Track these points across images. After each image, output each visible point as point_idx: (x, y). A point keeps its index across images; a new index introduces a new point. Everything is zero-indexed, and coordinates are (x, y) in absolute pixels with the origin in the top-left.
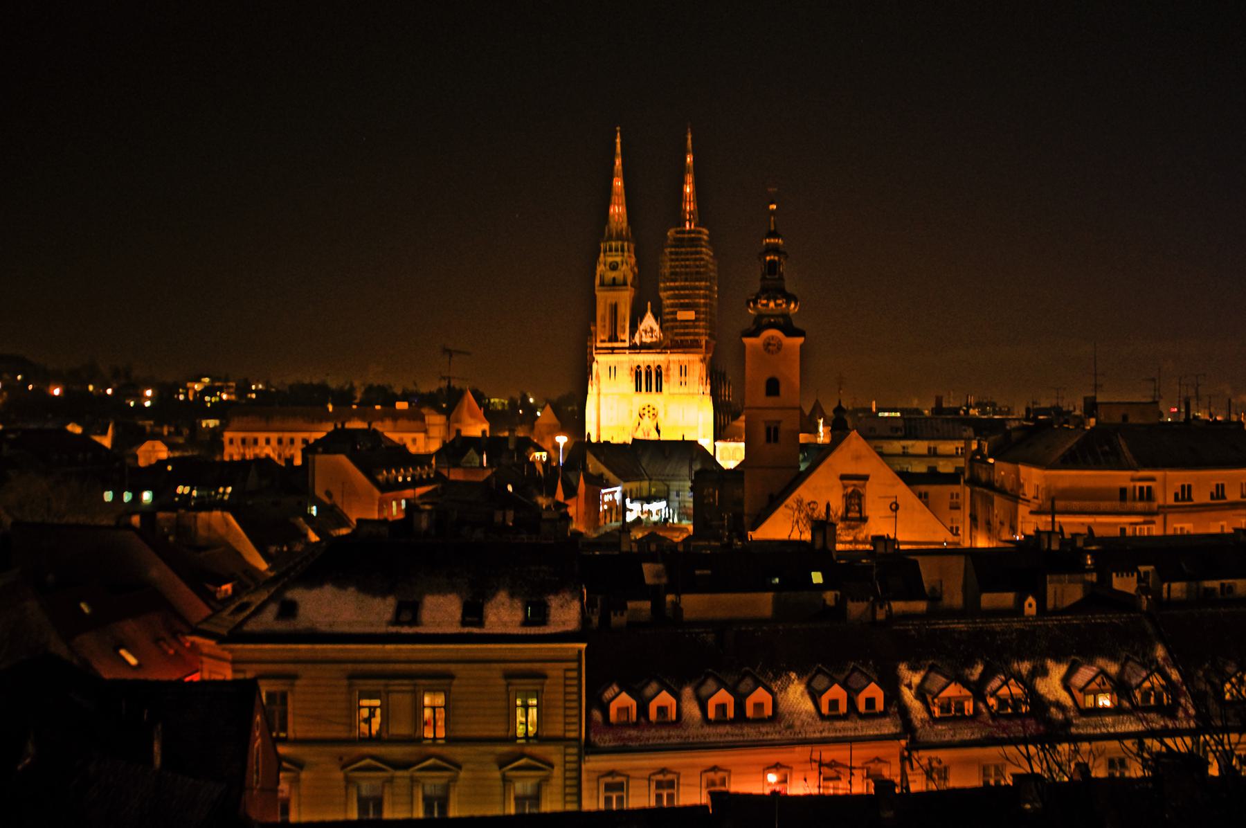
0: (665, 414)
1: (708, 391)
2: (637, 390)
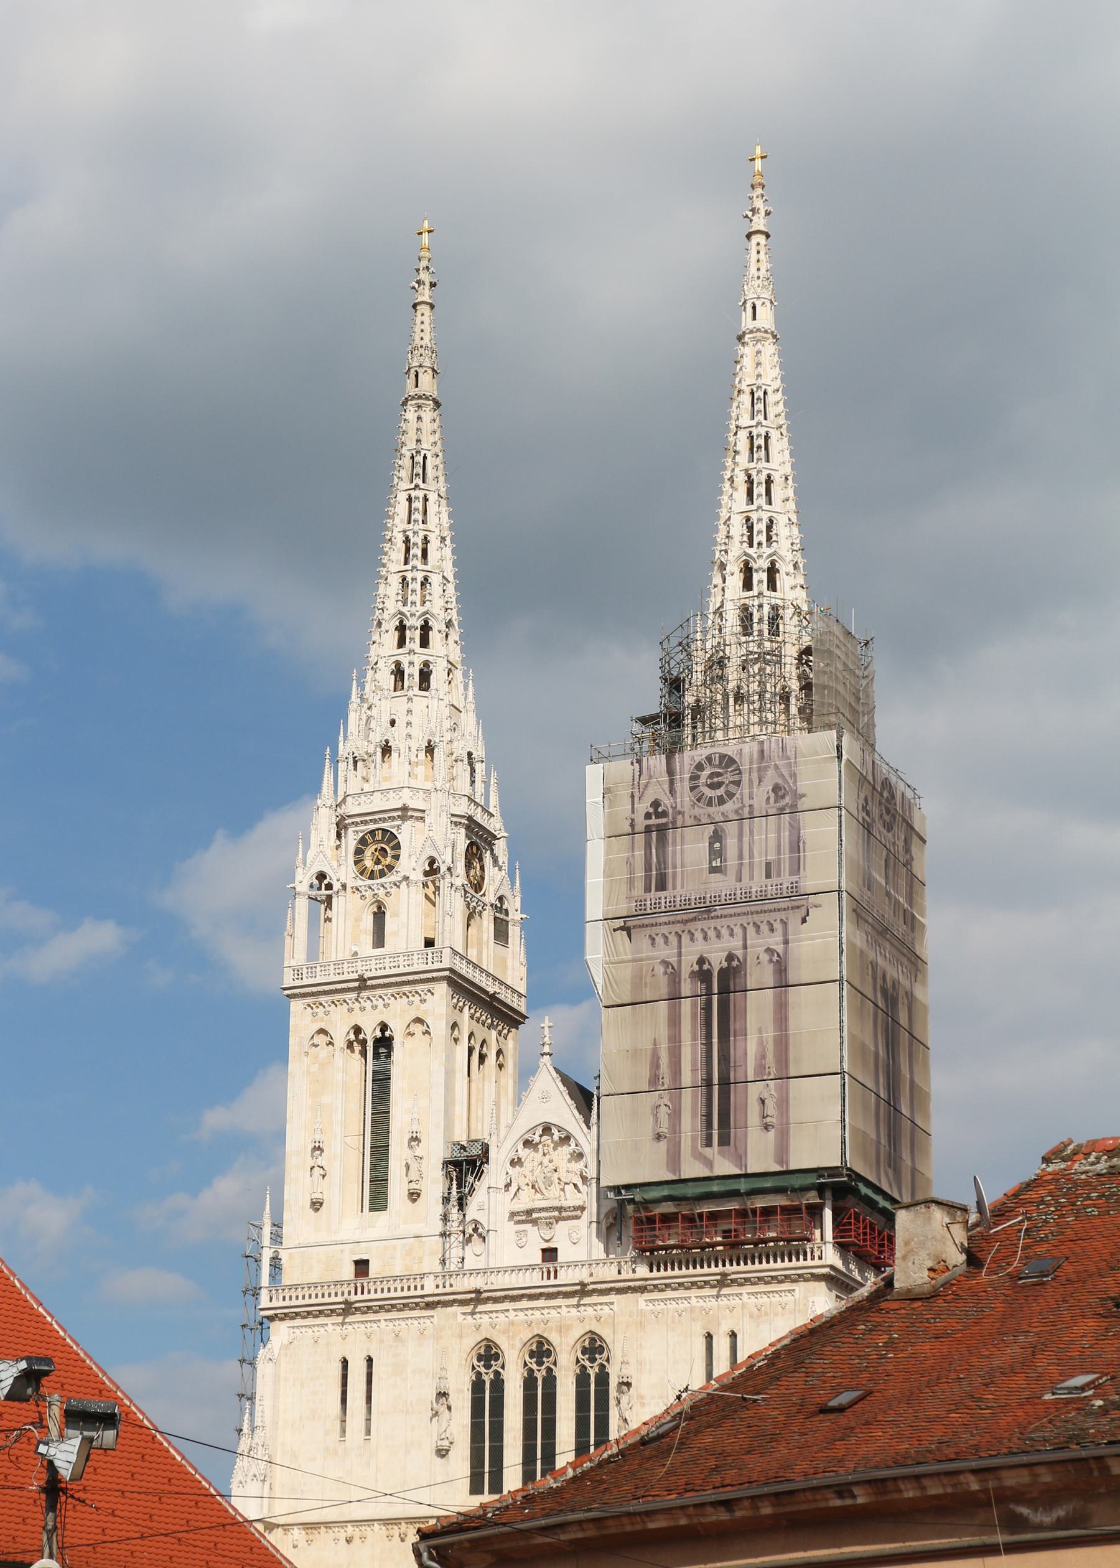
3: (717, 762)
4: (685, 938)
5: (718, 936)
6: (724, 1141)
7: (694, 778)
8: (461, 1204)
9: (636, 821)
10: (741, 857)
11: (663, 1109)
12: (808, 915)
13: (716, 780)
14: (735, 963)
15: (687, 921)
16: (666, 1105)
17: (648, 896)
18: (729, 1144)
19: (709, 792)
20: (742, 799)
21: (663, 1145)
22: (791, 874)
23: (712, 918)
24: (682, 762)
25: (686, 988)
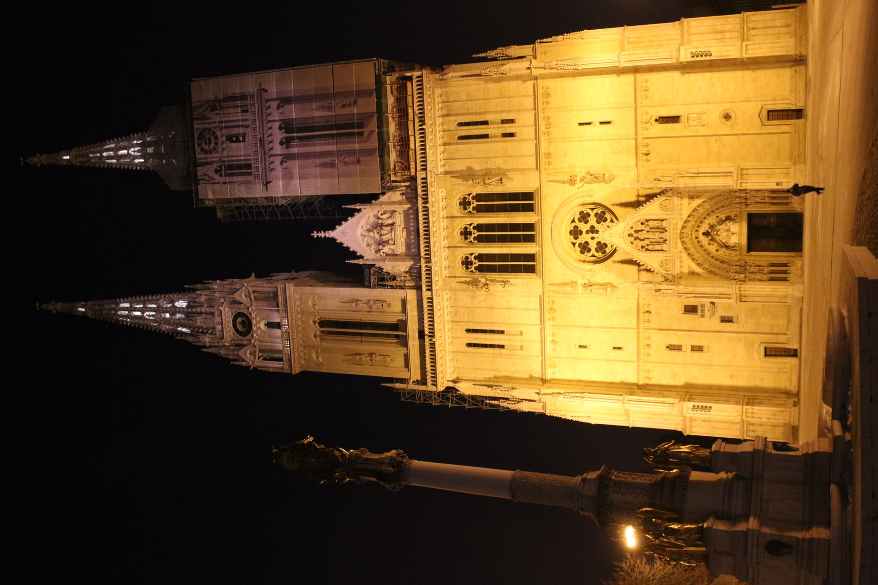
0: (595, 178)
1: (526, 50)
2: (531, 270)
3: (200, 141)
4: (272, 153)
5: (271, 135)
7: (206, 152)
8: (394, 278)
9: (223, 181)
11: (346, 160)
12: (264, 89)
13: (207, 141)
14: (283, 125)
15: (265, 152)
17: (254, 173)
19: (212, 145)
20: (215, 127)
21: (362, 159)
24: (200, 159)
25: (295, 150)
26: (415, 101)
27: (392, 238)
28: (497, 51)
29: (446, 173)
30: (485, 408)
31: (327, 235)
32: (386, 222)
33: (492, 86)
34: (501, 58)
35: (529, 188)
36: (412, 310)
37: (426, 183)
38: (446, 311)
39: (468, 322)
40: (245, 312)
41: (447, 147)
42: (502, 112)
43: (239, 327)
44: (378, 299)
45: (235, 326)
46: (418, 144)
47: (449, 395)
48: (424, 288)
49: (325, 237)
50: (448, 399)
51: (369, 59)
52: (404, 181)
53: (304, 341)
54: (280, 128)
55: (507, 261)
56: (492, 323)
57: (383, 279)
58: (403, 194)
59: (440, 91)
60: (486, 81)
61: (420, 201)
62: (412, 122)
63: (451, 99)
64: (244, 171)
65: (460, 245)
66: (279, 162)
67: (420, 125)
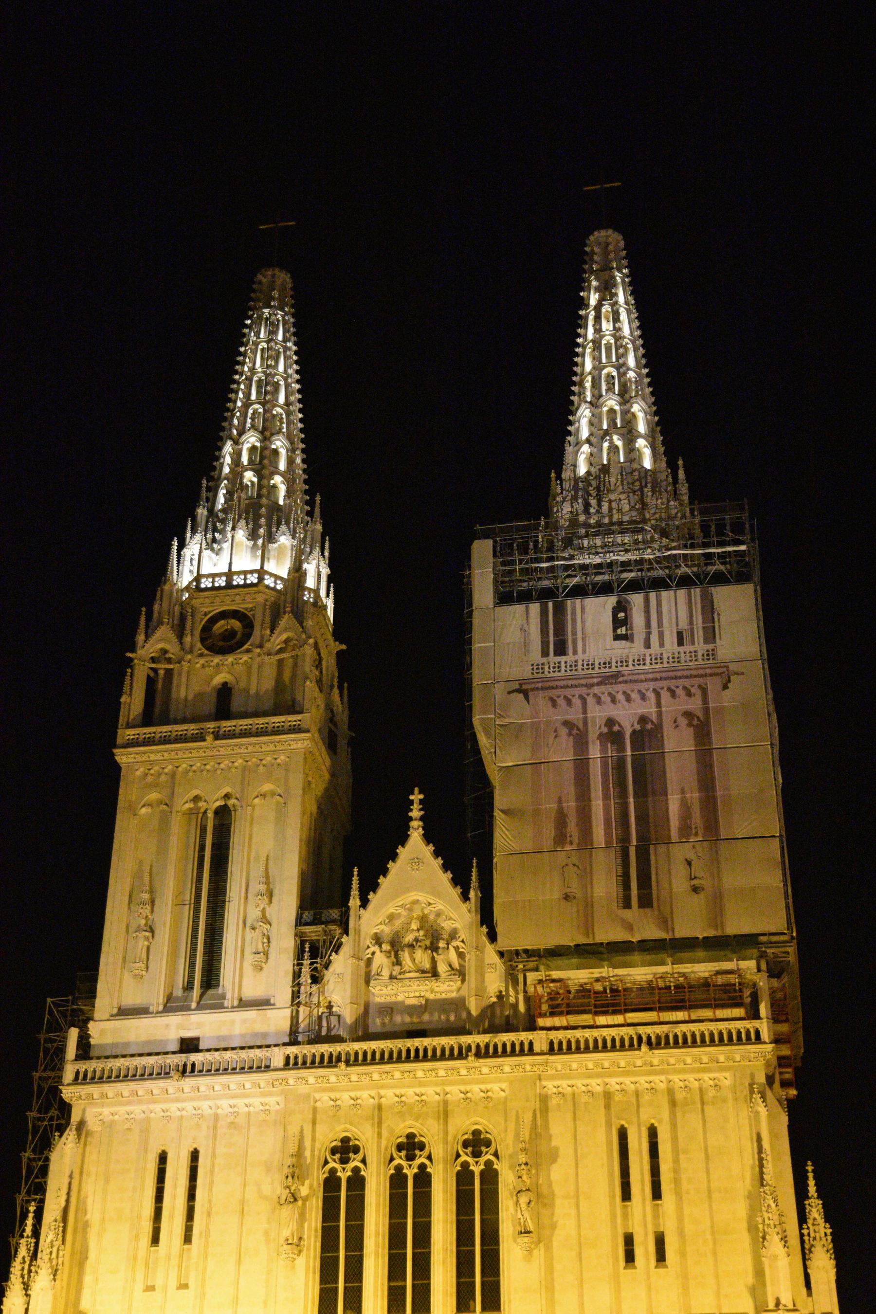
5: (628, 699)
6: (646, 902)
8: (316, 979)
10: (648, 625)
12: (729, 681)
14: (649, 726)
15: (590, 686)
16: (574, 865)
18: (652, 907)
22: (706, 641)
23: (620, 683)
25: (595, 751)
26: (704, 1027)
27: (404, 973)
28: (821, 1221)
29: (544, 1099)
30: (20, 1198)
31: (415, 824)
32: (439, 958)
33: (741, 1209)
34: (805, 1232)
35: (510, 1302)
36: (244, 1021)
37: (522, 1053)
38: (240, 1102)
39: (214, 1156)
40: (256, 637)
41: (602, 1102)
42: (681, 1234)
43: (221, 626)
44: (271, 940)
45: (223, 615)
46: (607, 1033)
47: (54, 1112)
48: (292, 1050)
49: (411, 819)
50: (45, 1109)
51: (793, 920)
52: (527, 999)
53: (186, 772)
54: (643, 720)
55: (347, 1249)
56: (209, 1214)
57: (315, 953)
58: (500, 997)
59: (727, 1083)
60: (750, 1196)
61: (481, 1039)
62: (656, 1019)
63: (710, 1110)
64: (551, 638)
65: (385, 1133)
66: (568, 717)
67: (649, 1038)
